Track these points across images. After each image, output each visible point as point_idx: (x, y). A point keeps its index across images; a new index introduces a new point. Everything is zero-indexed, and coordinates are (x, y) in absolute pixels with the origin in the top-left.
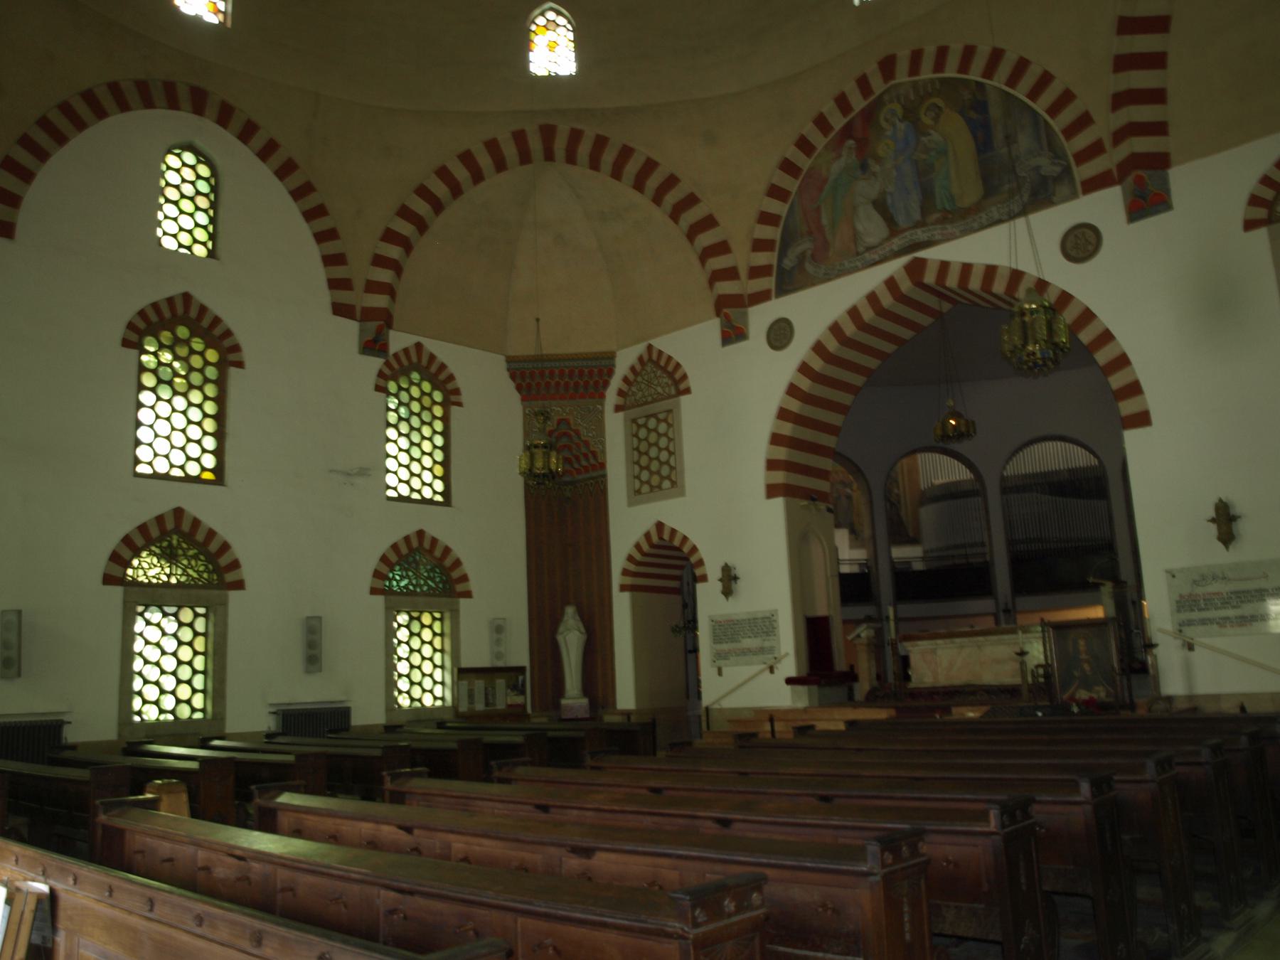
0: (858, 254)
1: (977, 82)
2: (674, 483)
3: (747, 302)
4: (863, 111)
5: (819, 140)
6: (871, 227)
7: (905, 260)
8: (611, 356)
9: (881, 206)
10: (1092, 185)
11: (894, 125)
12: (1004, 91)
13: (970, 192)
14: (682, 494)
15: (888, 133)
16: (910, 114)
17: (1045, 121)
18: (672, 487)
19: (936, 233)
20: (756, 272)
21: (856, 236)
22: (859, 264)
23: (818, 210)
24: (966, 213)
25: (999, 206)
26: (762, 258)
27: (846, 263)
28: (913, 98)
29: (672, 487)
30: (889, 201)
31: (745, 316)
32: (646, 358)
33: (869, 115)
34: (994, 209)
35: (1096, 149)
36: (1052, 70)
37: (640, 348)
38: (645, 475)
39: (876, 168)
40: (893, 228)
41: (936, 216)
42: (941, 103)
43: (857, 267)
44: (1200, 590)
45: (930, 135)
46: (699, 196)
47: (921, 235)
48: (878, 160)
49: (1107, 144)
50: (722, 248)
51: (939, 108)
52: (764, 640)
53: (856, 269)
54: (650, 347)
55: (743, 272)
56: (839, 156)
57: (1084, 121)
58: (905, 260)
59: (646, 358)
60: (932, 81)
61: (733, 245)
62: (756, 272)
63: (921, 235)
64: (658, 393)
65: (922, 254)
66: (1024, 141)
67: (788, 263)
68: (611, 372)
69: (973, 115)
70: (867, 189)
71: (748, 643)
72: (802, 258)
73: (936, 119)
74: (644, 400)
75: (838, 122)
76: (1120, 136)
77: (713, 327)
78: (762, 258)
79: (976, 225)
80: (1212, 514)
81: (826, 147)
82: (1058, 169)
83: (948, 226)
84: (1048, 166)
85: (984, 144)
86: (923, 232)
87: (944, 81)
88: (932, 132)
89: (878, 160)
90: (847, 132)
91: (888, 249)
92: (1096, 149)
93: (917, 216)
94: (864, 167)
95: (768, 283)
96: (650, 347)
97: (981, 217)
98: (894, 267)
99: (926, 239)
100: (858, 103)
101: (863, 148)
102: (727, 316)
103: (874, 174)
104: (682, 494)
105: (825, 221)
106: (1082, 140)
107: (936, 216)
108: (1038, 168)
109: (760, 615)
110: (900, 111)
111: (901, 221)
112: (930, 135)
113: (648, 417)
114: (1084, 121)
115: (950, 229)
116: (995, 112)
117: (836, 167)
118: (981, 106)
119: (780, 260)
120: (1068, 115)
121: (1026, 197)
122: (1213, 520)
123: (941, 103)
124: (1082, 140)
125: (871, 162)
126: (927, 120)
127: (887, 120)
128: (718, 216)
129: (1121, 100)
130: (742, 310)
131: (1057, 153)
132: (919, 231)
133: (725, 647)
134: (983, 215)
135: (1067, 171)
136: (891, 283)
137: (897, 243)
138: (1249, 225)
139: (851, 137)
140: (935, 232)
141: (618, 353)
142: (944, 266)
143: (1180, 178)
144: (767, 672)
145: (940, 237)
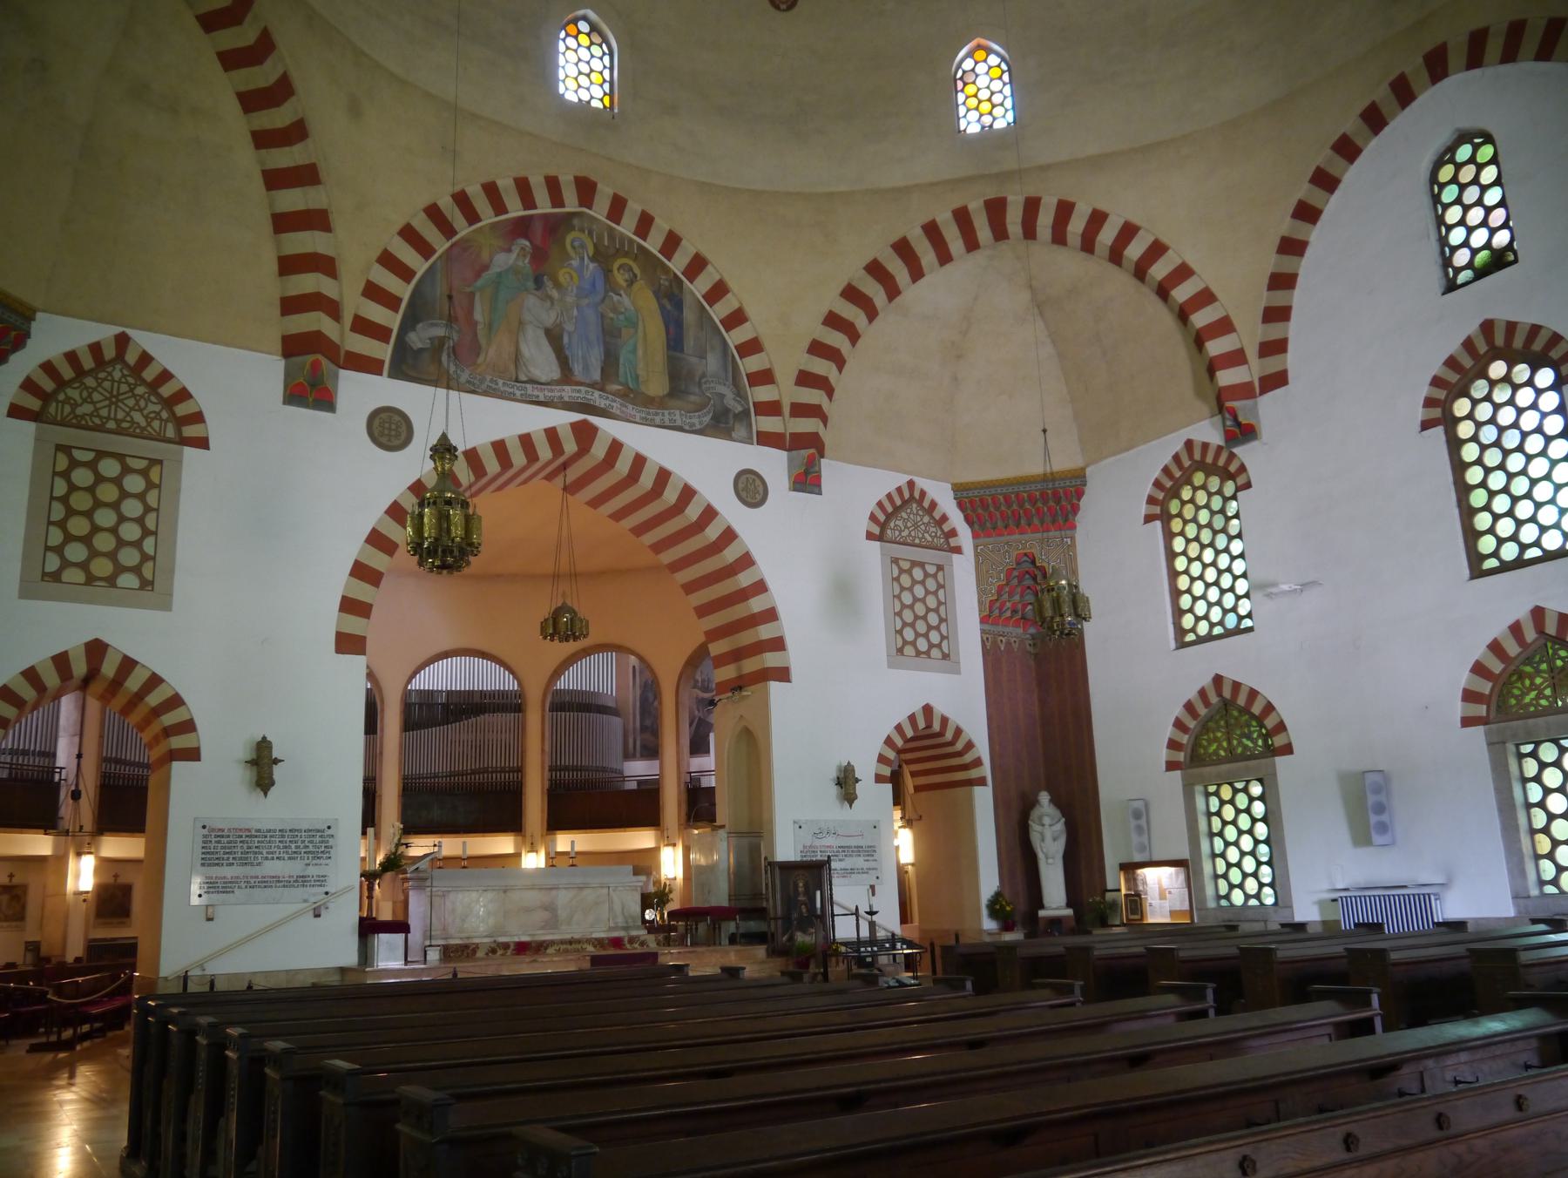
0: (517, 380)
1: (675, 274)
2: (146, 584)
3: (342, 362)
4: (545, 217)
5: (488, 217)
6: (542, 362)
7: (577, 417)
8: (28, 315)
9: (554, 337)
10: (766, 439)
11: (582, 259)
12: (700, 302)
13: (657, 386)
14: (165, 605)
15: (575, 263)
16: (603, 257)
17: (733, 356)
18: (142, 588)
19: (616, 407)
20: (363, 326)
21: (517, 357)
22: (518, 393)
23: (471, 296)
24: (648, 402)
25: (683, 412)
26: (377, 313)
27: (501, 382)
28: (606, 243)
29: (142, 588)
30: (566, 339)
31: (336, 376)
32: (109, 353)
33: (556, 226)
34: (677, 412)
35: (772, 409)
36: (750, 311)
37: (104, 333)
38: (76, 552)
39: (555, 294)
40: (567, 377)
41: (616, 387)
42: (637, 271)
43: (514, 395)
44: (818, 843)
45: (621, 296)
46: (323, 175)
47: (597, 398)
48: (557, 285)
49: (786, 410)
50: (325, 265)
51: (635, 276)
52: (308, 865)
53: (511, 398)
54: (122, 341)
55: (348, 320)
56: (509, 250)
57: (764, 377)
58: (577, 417)
59: (109, 353)
60: (631, 241)
61: (342, 269)
62: (363, 326)
63: (597, 398)
64: (132, 422)
65: (595, 420)
66: (712, 363)
67: (416, 339)
68: (20, 342)
69: (669, 307)
70: (537, 311)
71: (272, 868)
72: (438, 345)
73: (631, 282)
74: (97, 421)
75: (515, 210)
76: (800, 410)
77: (271, 371)
78: (377, 313)
79: (658, 420)
80: (249, 755)
81: (494, 226)
82: (739, 409)
83: (630, 407)
84: (731, 401)
85: (675, 342)
86: (600, 396)
87: (641, 247)
88: (622, 292)
89: (557, 285)
90: (521, 228)
91: (558, 394)
92: (772, 409)
93: (596, 376)
94: (538, 283)
95: (384, 352)
96: (122, 341)
97: (663, 415)
98: (562, 419)
99: (602, 406)
100: (544, 206)
101: (539, 257)
102: (316, 366)
103: (551, 299)
104: (165, 605)
105: (478, 315)
106: (763, 394)
107: (616, 387)
108: (722, 396)
109: (305, 826)
110: (591, 250)
111: (577, 369)
112: (621, 296)
113: (101, 454)
114: (764, 377)
115: (630, 410)
116: (689, 316)
117: (503, 261)
118: (679, 305)
119: (407, 326)
120: (752, 364)
121: (707, 419)
122: (276, 761)
123: (637, 271)
124: (763, 394)
125: (549, 284)
126: (620, 278)
127: (573, 247)
128: (336, 220)
129: (806, 379)
130: (332, 367)
131: (740, 394)
132: (597, 393)
133: (228, 872)
134: (666, 412)
135: (746, 413)
136: (551, 434)
137: (568, 393)
138: (870, 536)
139: (526, 237)
140: (614, 404)
141: (39, 315)
142: (616, 447)
143: (827, 467)
144: (311, 913)
145: (618, 412)
